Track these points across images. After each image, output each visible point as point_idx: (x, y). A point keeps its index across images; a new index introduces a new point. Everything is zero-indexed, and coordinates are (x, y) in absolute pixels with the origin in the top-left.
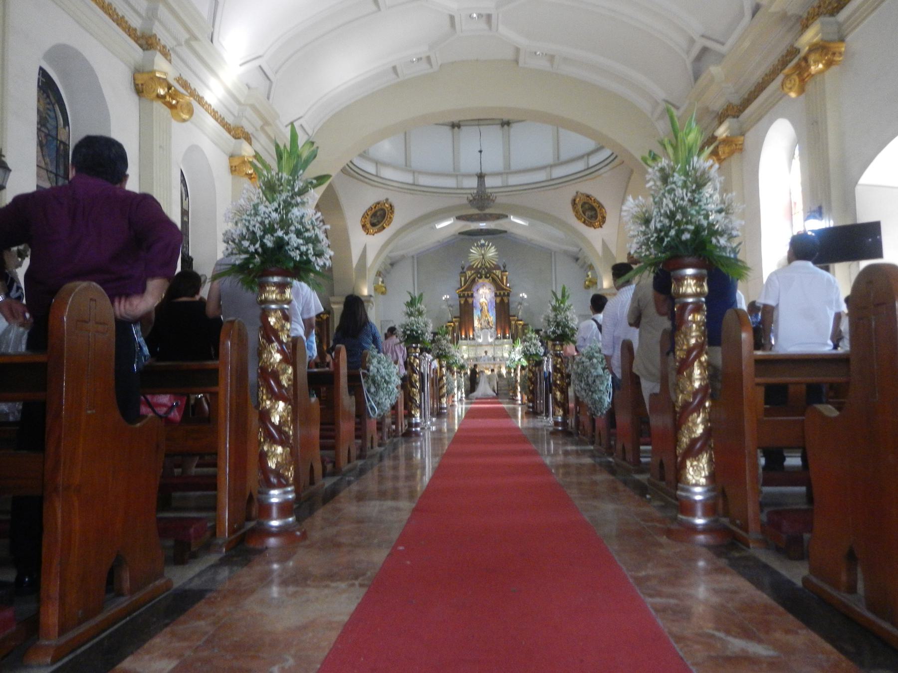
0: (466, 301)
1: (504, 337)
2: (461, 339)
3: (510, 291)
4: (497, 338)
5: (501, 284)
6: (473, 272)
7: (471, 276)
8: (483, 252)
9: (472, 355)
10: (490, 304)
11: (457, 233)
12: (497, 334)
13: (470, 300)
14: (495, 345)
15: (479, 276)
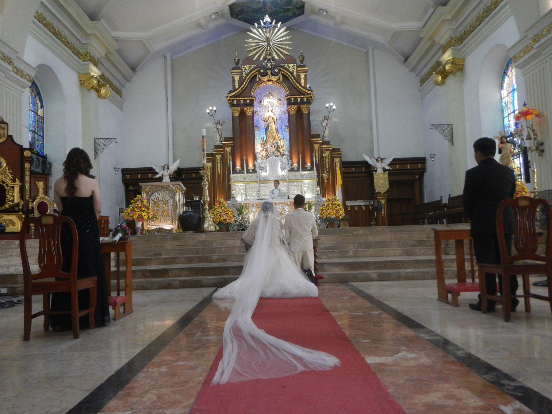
0: (242, 113)
1: (304, 169)
2: (235, 171)
3: (311, 97)
4: (292, 170)
5: (299, 86)
6: (252, 66)
7: (250, 72)
8: (268, 34)
9: (253, 197)
10: (279, 122)
11: (227, 10)
12: (292, 165)
13: (248, 111)
14: (290, 180)
15: (262, 71)
